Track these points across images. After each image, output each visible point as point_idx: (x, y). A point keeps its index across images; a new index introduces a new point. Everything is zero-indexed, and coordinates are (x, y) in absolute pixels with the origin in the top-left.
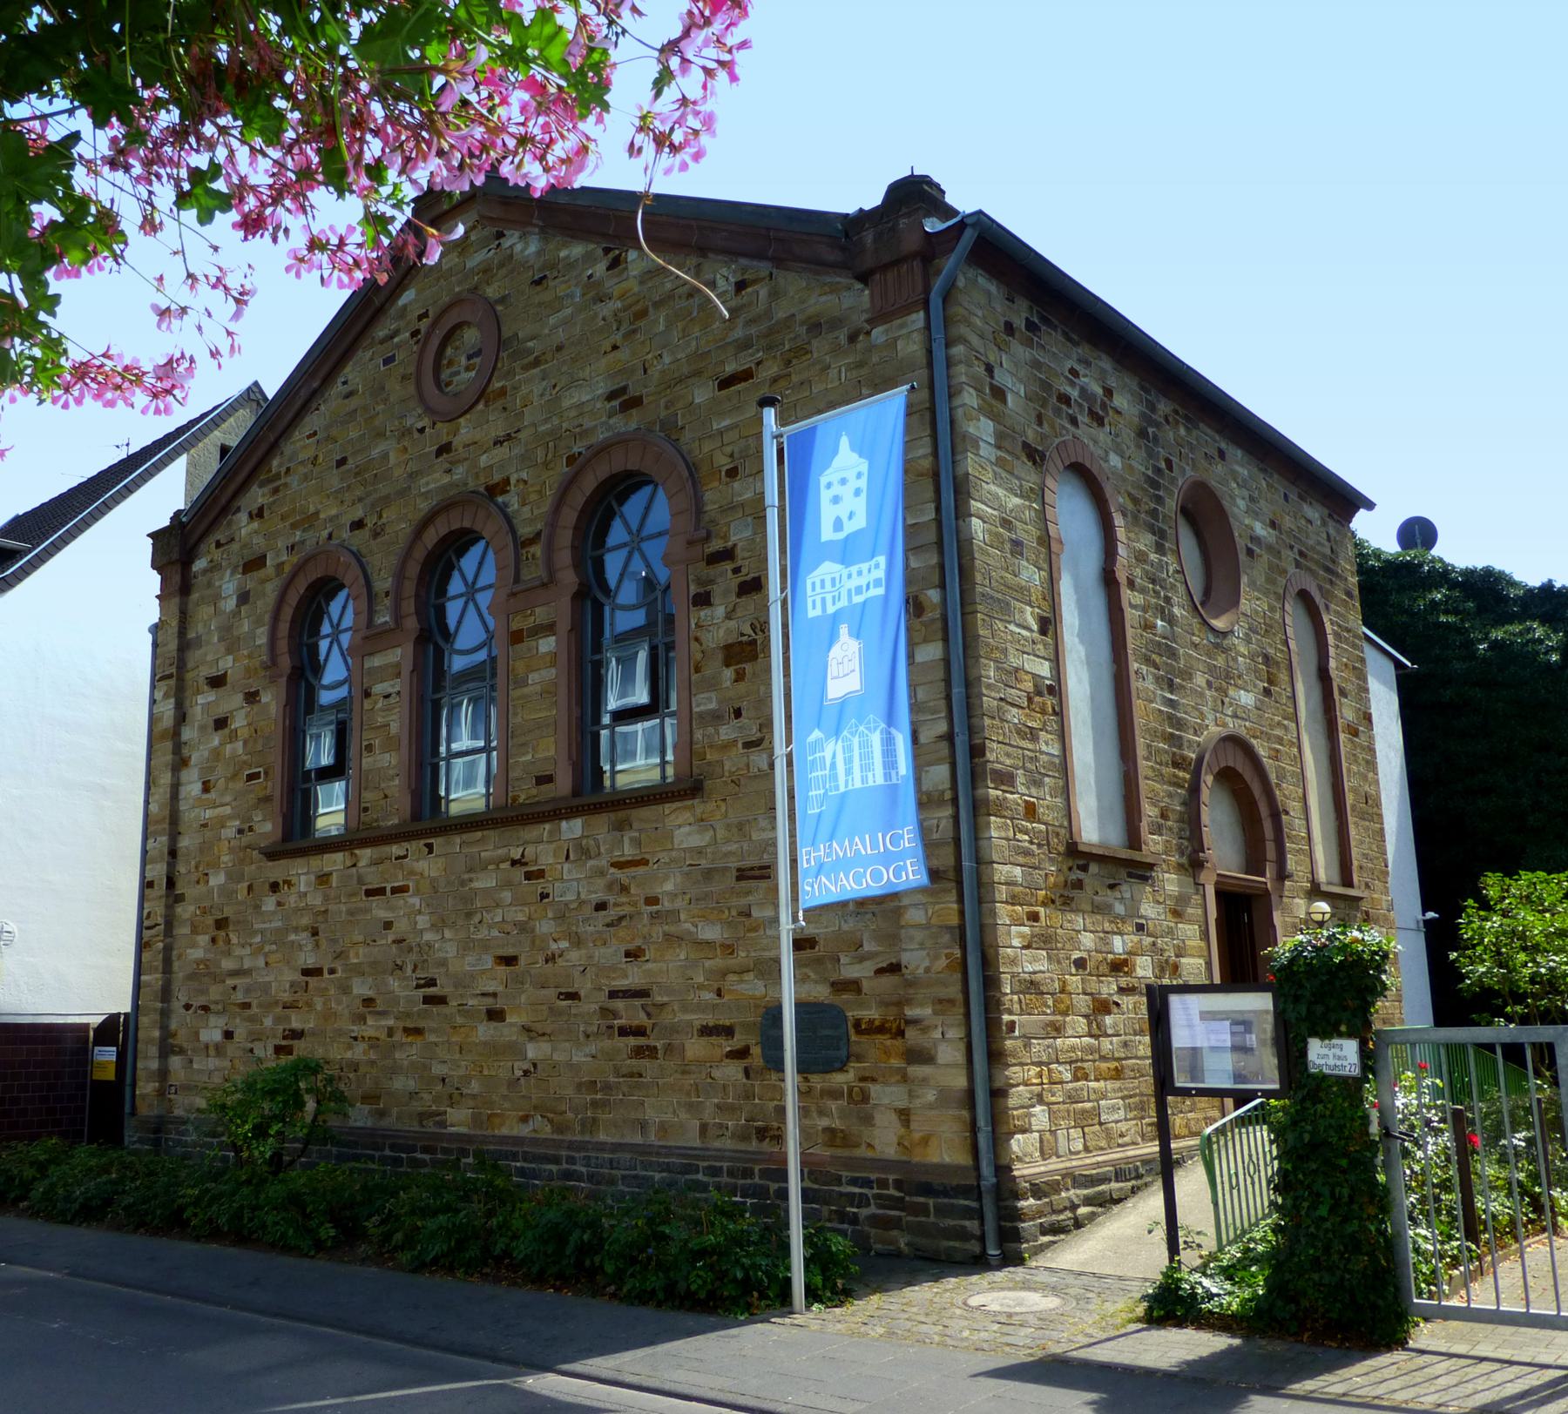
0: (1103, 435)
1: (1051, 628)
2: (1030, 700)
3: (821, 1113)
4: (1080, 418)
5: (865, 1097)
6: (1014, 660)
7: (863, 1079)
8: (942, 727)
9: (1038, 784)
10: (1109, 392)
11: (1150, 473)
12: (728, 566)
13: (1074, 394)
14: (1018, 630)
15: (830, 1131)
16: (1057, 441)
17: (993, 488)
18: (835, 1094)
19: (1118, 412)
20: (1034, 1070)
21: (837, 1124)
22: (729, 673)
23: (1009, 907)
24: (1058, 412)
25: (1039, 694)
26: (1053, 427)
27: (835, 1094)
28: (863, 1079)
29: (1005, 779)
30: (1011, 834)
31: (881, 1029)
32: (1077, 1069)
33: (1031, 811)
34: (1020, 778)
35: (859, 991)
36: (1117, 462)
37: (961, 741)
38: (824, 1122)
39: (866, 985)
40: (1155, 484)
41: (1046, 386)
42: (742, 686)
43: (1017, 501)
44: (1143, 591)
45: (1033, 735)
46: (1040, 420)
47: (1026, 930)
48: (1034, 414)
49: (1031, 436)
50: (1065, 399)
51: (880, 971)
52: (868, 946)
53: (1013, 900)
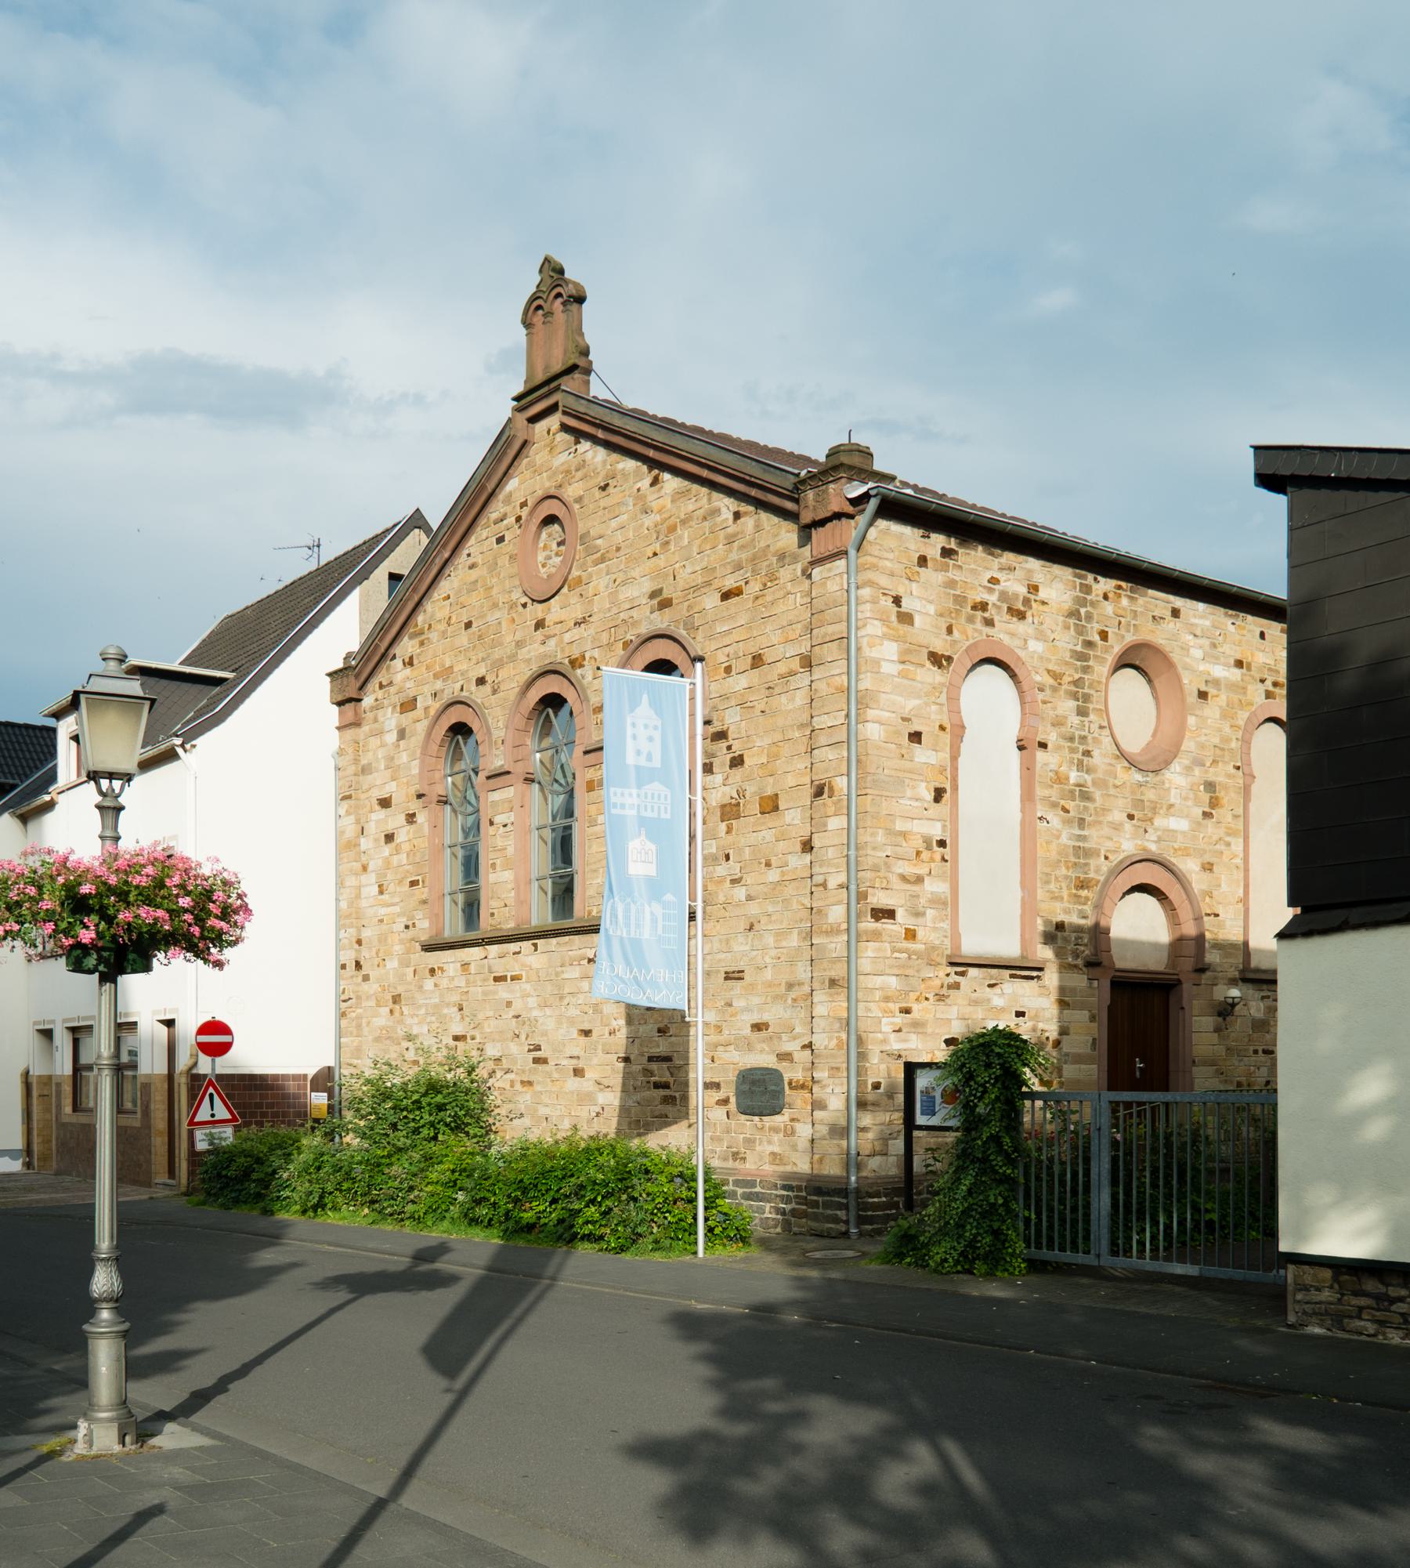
0: (1020, 627)
1: (947, 796)
2: (918, 853)
3: (770, 1142)
4: (996, 619)
5: (793, 1133)
6: (900, 826)
7: (793, 1120)
8: (842, 878)
9: (918, 914)
10: (1034, 588)
11: (1079, 648)
12: (723, 744)
13: (992, 599)
15: (773, 1154)
16: (968, 643)
17: (892, 697)
18: (775, 1130)
19: (1044, 603)
21: (776, 1149)
22: (723, 826)
24: (971, 620)
25: (929, 848)
26: (964, 632)
27: (775, 1130)
28: (793, 1120)
31: (803, 1087)
33: (911, 935)
34: (900, 914)
35: (792, 1061)
36: (1040, 643)
37: (853, 887)
38: (770, 1149)
39: (796, 1056)
40: (1082, 657)
42: (730, 838)
43: (913, 703)
44: (1059, 748)
45: (919, 880)
46: (950, 630)
49: (940, 646)
50: (983, 606)
51: (804, 1047)
52: (798, 1030)
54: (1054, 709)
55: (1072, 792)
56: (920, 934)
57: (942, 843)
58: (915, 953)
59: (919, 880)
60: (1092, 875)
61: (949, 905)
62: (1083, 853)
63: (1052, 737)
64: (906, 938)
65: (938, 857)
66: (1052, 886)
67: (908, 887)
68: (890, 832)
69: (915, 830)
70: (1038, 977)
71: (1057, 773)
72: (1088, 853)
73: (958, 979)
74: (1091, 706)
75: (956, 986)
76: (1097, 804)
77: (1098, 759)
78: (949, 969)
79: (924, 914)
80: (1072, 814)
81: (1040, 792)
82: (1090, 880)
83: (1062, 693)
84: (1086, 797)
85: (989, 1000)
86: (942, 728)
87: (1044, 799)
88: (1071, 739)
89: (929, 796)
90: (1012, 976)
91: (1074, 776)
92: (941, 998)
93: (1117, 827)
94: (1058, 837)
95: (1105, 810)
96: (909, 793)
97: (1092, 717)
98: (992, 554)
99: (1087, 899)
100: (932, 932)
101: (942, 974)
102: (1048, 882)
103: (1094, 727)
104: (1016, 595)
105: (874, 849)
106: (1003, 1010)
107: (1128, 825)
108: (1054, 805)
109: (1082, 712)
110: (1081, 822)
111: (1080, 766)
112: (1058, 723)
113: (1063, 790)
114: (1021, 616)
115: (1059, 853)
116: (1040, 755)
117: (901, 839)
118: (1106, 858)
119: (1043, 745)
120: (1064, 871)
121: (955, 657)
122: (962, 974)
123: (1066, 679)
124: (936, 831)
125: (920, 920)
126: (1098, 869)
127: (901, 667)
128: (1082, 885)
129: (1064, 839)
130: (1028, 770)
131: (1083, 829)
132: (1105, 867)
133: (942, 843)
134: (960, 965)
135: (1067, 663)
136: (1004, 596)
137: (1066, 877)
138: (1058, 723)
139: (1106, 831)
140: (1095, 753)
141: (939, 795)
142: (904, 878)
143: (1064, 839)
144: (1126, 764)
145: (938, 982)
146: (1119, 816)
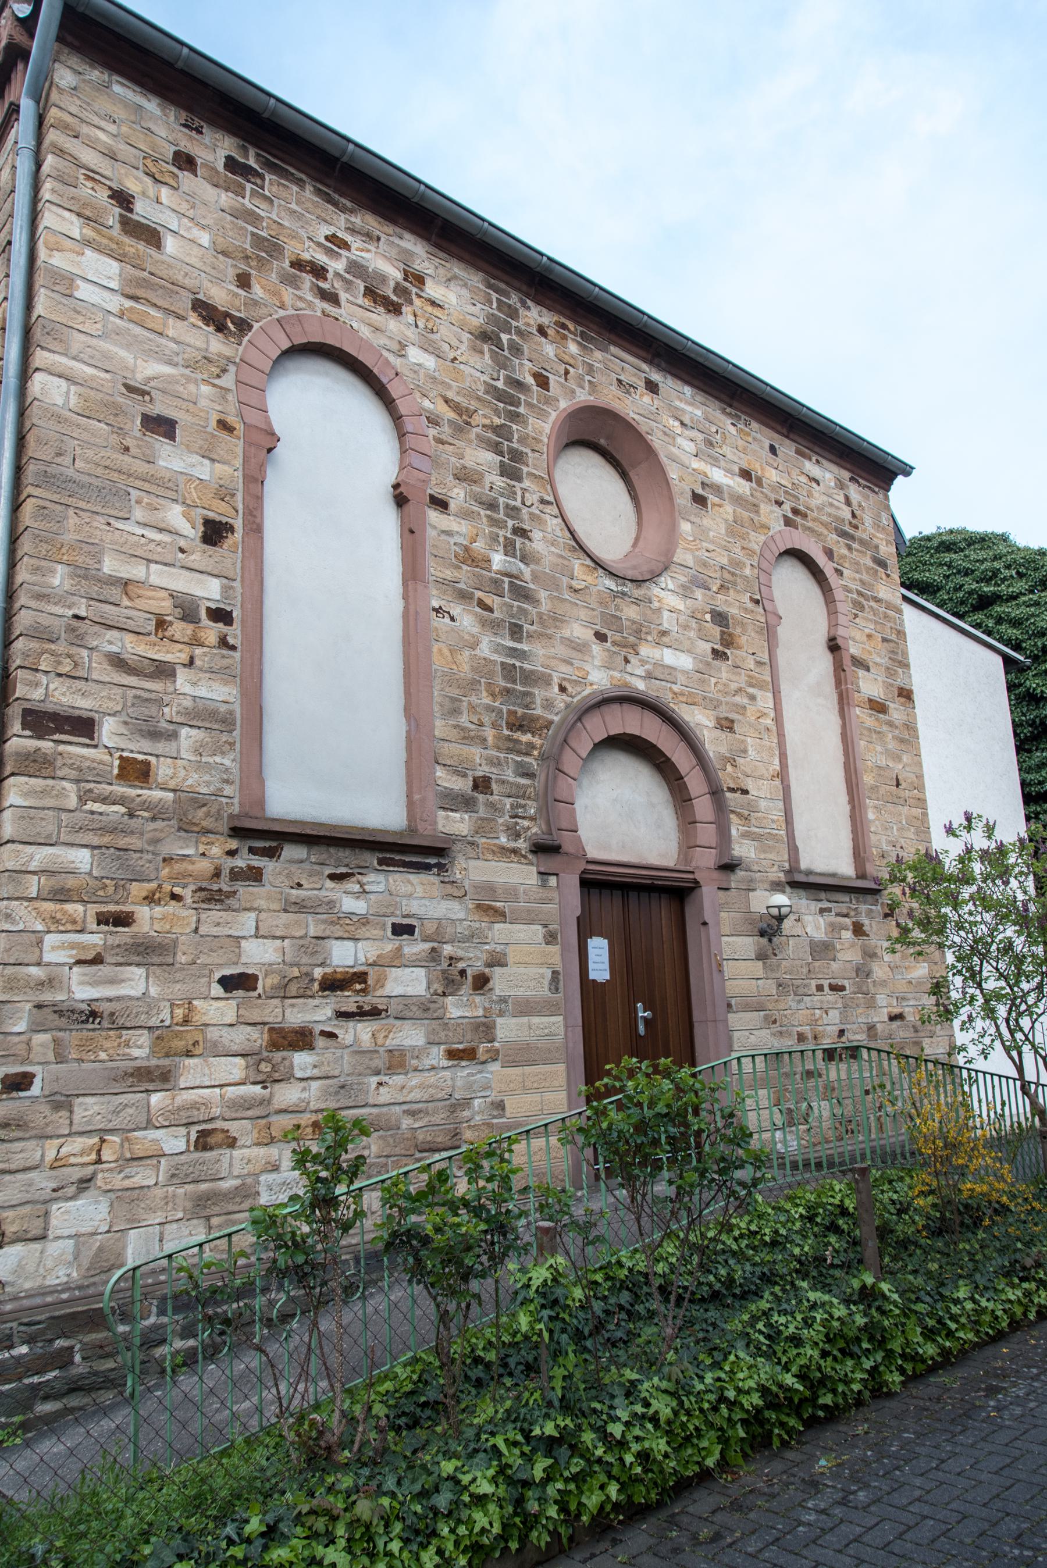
2: (161, 624)
6: (110, 566)
14: (139, 531)
20: (79, 1143)
23: (49, 906)
29: (83, 727)
30: (72, 802)
32: (203, 1134)
33: (137, 771)
41: (270, 247)
47: (97, 939)
48: (231, 273)
53: (61, 895)
54: (461, 457)
55: (496, 582)
56: (163, 770)
57: (221, 616)
58: (146, 806)
59: (164, 671)
60: (538, 711)
61: (243, 726)
62: (517, 678)
63: (457, 495)
64: (119, 776)
65: (212, 638)
66: (464, 720)
67: (132, 680)
68: (83, 574)
69: (154, 580)
70: (441, 867)
71: (467, 549)
72: (529, 678)
73: (257, 862)
74: (525, 469)
75: (255, 875)
76: (545, 606)
77: (538, 544)
78: (233, 844)
79: (173, 736)
80: (496, 614)
81: (434, 570)
82: (534, 719)
83: (473, 436)
84: (521, 593)
85: (331, 904)
86: (224, 425)
87: (441, 583)
88: (492, 506)
89: (192, 532)
90: (381, 862)
91: (498, 560)
92: (212, 897)
93: (581, 648)
94: (474, 645)
95: (557, 620)
96: (138, 514)
97: (527, 483)
98: (330, 201)
99: (531, 746)
100: (185, 765)
101: (216, 850)
102: (455, 712)
103: (532, 498)
104: (383, 278)
105: (39, 597)
106: (364, 921)
107: (596, 648)
108: (464, 596)
109: (510, 472)
110: (516, 632)
111: (509, 548)
112: (465, 476)
113: (478, 576)
114: (395, 309)
115: (474, 669)
116: (433, 516)
117: (114, 593)
118: (563, 689)
119: (440, 504)
120: (487, 700)
121: (256, 326)
122: (271, 853)
123: (478, 419)
124: (209, 591)
125: (161, 747)
126: (550, 704)
127: (128, 303)
128: (519, 724)
129: (485, 649)
130: (411, 535)
131: (519, 640)
132: (561, 701)
133: (221, 616)
134: (264, 837)
135: (479, 399)
136: (356, 268)
137: (490, 709)
138: (465, 476)
139: (561, 651)
140: (536, 534)
141: (214, 533)
142: (118, 662)
143: (485, 649)
144: (588, 562)
145: (204, 866)
146: (580, 632)
